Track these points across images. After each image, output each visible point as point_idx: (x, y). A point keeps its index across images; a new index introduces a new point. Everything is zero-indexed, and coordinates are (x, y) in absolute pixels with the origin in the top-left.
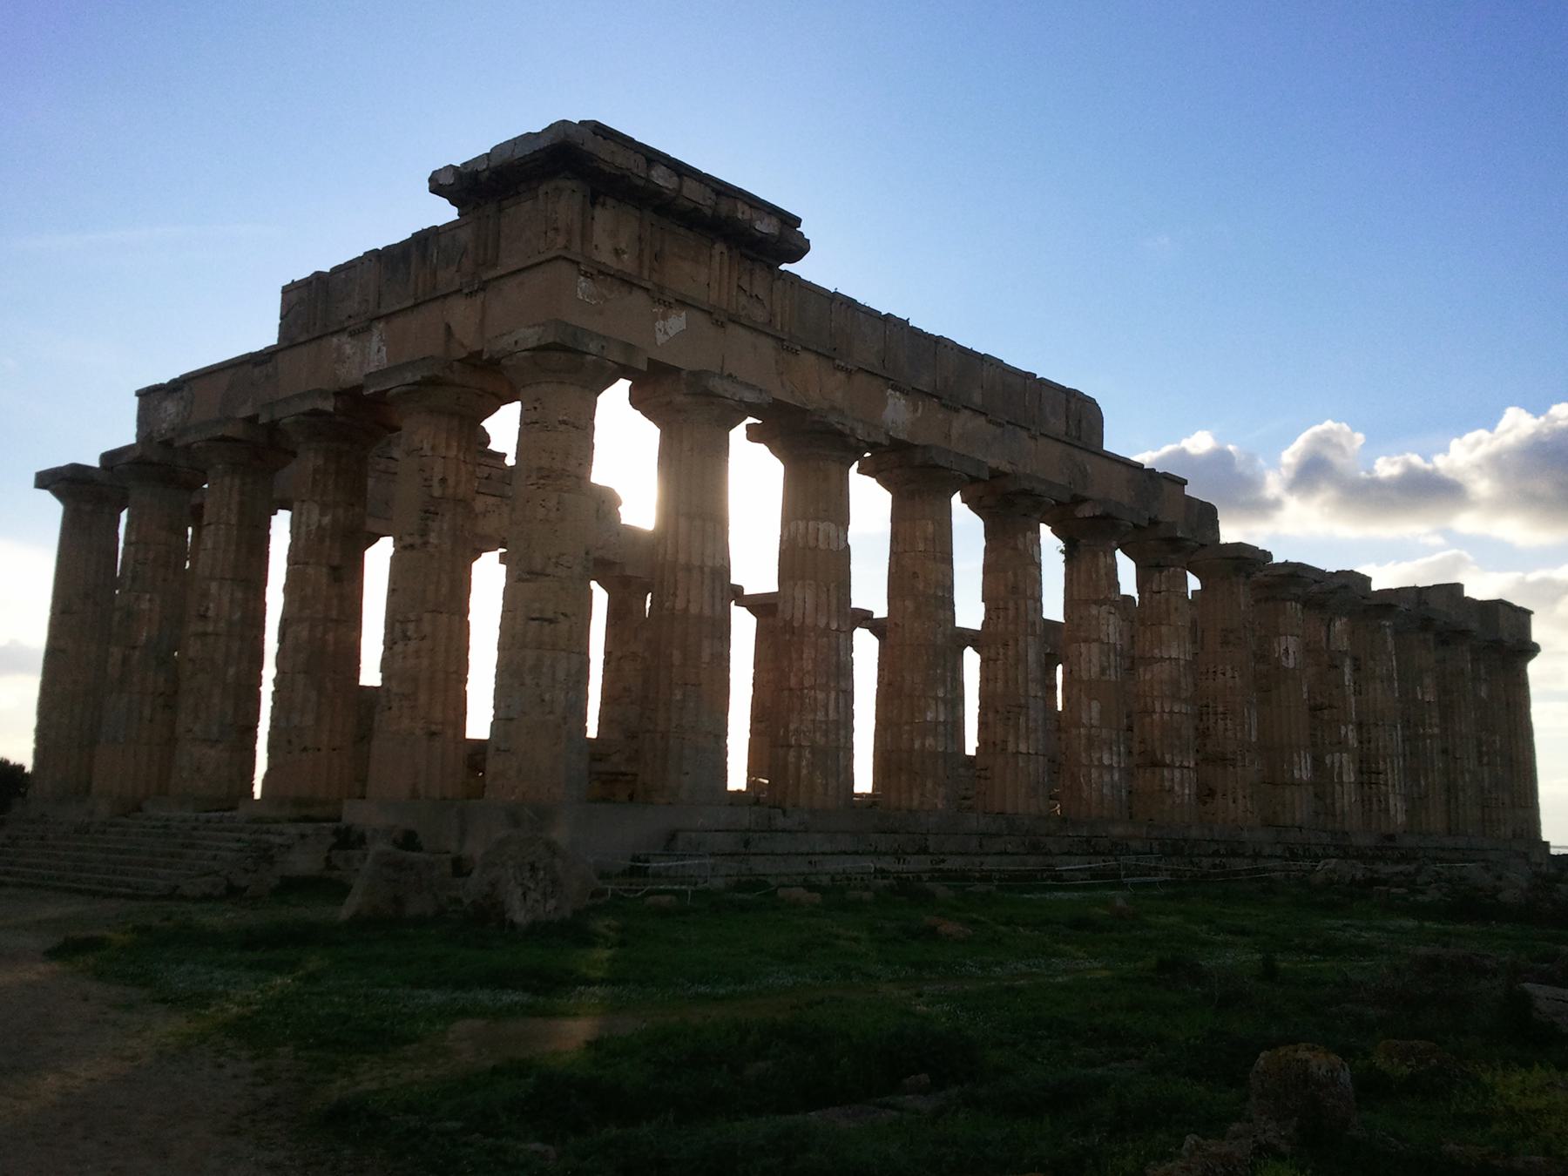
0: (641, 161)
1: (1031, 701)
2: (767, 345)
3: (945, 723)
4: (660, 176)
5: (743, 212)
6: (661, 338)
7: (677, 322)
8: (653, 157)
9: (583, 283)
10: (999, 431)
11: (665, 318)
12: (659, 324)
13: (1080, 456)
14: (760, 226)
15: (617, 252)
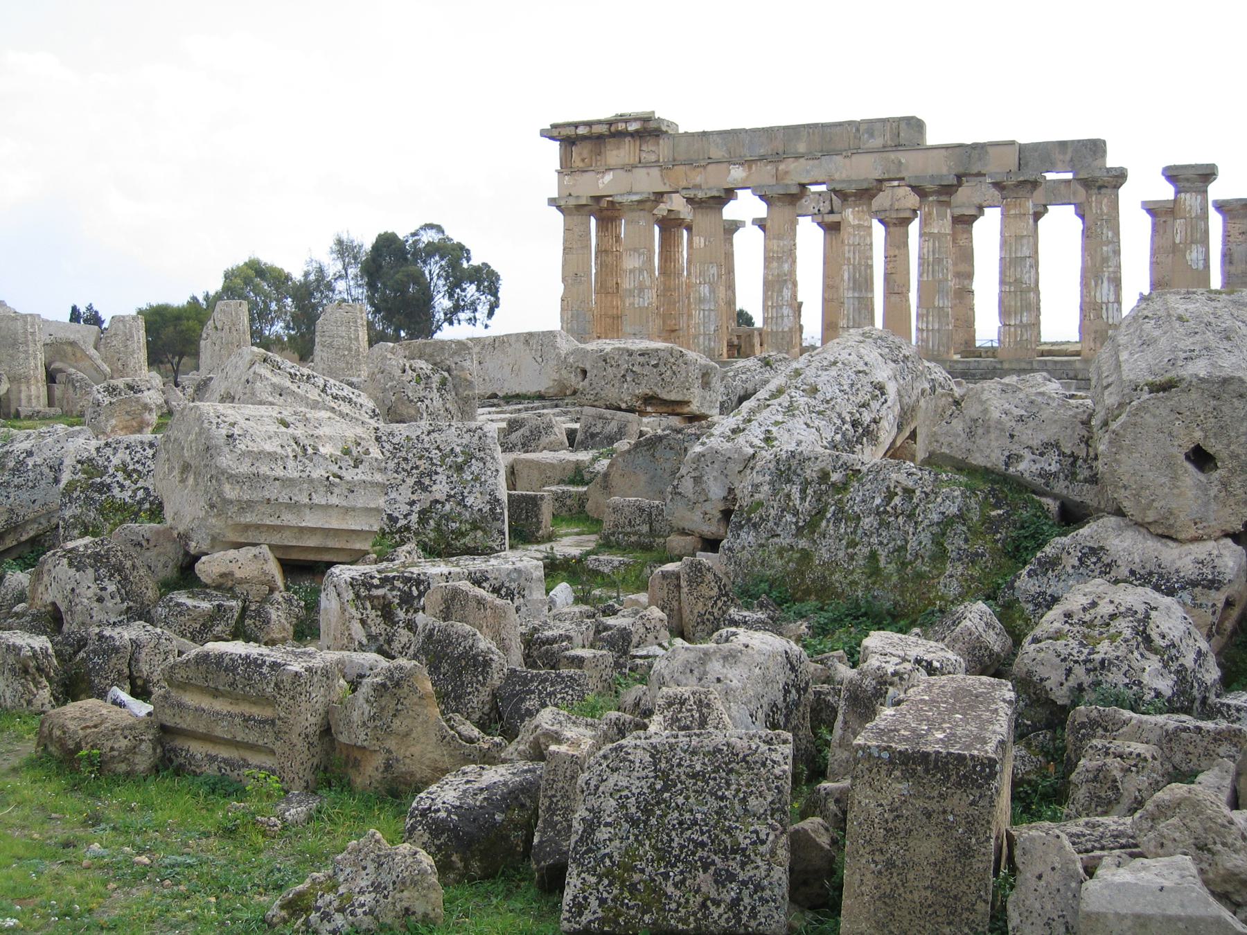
0: (574, 128)
1: (846, 300)
2: (655, 172)
3: (772, 318)
4: (582, 131)
5: (621, 126)
6: (601, 186)
7: (609, 177)
8: (576, 125)
9: (566, 178)
10: (816, 162)
11: (603, 177)
12: (601, 181)
13: (892, 156)
14: (629, 129)
15: (583, 160)
